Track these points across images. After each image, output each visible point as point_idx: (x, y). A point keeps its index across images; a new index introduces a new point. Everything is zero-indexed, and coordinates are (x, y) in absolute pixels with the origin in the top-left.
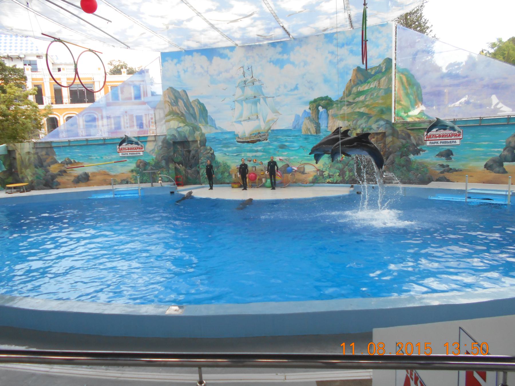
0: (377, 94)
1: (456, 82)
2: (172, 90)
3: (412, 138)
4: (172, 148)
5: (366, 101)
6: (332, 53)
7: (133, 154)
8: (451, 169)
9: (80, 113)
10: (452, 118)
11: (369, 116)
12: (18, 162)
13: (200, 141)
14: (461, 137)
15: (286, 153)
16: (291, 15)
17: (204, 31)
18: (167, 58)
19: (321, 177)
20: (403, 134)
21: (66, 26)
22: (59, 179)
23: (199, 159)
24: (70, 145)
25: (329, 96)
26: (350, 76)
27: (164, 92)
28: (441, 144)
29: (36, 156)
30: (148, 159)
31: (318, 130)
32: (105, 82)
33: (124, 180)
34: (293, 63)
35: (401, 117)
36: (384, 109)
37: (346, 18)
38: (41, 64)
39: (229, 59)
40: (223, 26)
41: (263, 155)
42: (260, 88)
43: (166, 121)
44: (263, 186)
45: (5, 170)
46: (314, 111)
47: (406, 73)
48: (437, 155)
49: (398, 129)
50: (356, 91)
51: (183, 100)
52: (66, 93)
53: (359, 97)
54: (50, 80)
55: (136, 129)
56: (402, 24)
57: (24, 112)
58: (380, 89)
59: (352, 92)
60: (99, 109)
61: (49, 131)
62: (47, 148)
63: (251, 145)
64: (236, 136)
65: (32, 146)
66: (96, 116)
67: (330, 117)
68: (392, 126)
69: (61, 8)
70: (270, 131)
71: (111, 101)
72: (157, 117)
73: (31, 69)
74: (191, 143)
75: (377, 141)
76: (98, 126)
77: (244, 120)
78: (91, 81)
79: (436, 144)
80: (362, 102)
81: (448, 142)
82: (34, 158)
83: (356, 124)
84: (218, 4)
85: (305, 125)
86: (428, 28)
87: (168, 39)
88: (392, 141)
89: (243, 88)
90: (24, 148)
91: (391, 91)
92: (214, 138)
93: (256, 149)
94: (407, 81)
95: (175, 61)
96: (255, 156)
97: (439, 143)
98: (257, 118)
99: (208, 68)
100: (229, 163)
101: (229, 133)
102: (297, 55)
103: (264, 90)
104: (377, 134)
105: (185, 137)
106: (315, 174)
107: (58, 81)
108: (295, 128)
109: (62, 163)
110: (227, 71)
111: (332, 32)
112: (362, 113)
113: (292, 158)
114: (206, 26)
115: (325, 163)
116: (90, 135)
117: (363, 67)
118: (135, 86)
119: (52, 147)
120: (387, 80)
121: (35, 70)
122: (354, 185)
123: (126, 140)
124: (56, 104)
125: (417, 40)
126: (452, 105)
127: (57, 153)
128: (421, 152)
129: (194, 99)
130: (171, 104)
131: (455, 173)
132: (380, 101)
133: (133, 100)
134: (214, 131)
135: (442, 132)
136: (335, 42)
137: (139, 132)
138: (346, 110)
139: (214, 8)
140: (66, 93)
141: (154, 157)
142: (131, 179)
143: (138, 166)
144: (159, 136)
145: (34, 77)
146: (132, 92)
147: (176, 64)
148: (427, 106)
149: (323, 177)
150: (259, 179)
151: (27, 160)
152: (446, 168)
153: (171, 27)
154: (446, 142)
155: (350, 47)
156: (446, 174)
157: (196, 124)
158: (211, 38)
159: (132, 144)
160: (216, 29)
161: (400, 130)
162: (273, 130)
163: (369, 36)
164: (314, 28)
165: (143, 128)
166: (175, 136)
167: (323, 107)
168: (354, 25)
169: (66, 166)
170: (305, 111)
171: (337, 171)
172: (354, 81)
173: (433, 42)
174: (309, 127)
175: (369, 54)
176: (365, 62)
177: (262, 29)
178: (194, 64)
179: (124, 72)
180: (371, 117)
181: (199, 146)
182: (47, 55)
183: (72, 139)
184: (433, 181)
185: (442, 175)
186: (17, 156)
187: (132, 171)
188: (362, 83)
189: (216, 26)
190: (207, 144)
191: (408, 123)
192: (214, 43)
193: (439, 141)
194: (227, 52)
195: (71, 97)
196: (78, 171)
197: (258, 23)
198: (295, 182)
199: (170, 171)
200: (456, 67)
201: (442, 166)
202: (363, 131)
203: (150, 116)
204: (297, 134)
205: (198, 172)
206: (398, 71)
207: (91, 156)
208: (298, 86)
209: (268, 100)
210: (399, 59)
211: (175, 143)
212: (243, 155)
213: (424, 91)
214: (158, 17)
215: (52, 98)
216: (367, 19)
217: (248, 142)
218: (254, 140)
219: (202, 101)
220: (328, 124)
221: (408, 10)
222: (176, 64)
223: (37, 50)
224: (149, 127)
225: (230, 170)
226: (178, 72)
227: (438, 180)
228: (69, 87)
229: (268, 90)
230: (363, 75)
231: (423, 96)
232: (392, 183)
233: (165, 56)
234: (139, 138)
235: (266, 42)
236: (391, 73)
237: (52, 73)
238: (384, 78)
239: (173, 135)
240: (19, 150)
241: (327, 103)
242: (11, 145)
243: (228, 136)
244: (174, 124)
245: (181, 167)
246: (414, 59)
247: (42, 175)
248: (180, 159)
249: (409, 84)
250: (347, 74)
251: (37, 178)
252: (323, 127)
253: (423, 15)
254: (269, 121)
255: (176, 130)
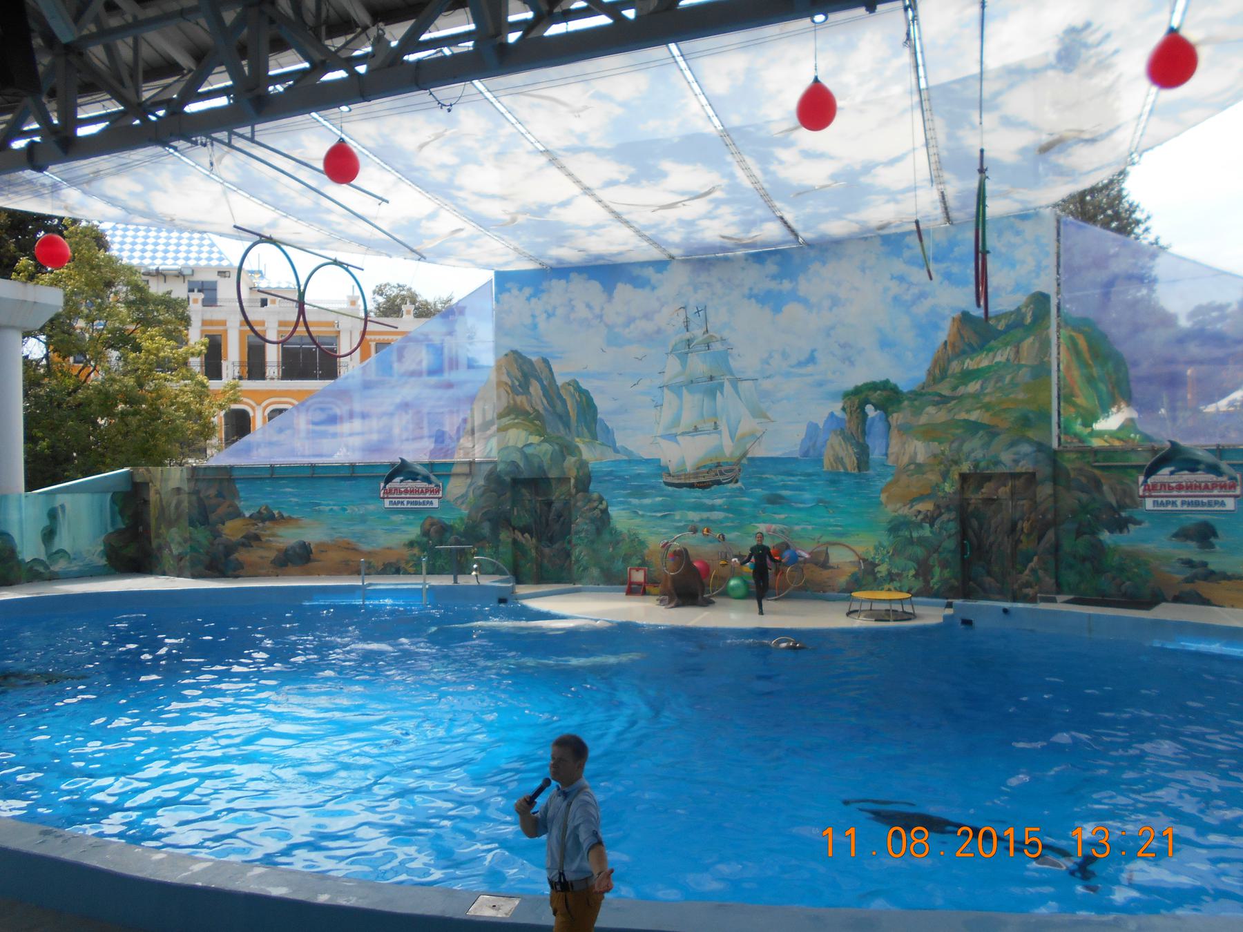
0: (1013, 379)
1: (1219, 353)
2: (516, 357)
3: (1105, 488)
4: (508, 494)
5: (985, 395)
6: (901, 279)
7: (416, 503)
8: (1212, 573)
9: (302, 404)
10: (1214, 442)
11: (991, 432)
12: (153, 511)
13: (576, 479)
14: (1238, 492)
15: (782, 516)
16: (802, 194)
17: (599, 226)
18: (508, 286)
19: (870, 578)
20: (1083, 480)
21: (288, 212)
22: (241, 555)
23: (570, 523)
24: (273, 475)
25: (893, 381)
26: (943, 335)
27: (498, 361)
28: (1185, 508)
29: (194, 498)
30: (448, 518)
31: (863, 460)
32: (364, 333)
33: (390, 564)
34: (804, 301)
35: (1076, 435)
36: (1031, 415)
37: (933, 202)
38: (226, 290)
39: (654, 288)
40: (643, 218)
41: (726, 518)
42: (724, 357)
43: (499, 430)
44: (725, 594)
45: (121, 525)
46: (854, 416)
47: (1086, 329)
48: (1176, 535)
49: (1068, 466)
50: (958, 370)
51: (540, 381)
52: (273, 354)
53: (966, 384)
54: (241, 325)
55: (429, 444)
56: (1072, 213)
57: (177, 396)
58: (1020, 367)
59: (950, 372)
60: (344, 394)
61: (229, 441)
62: (221, 480)
63: (698, 492)
64: (662, 469)
65: (185, 475)
66: (338, 411)
67: (894, 432)
68: (1054, 457)
69: (282, 172)
70: (744, 461)
71: (372, 376)
72: (478, 421)
73: (204, 300)
74: (553, 483)
75: (1013, 493)
76: (342, 435)
77: (683, 434)
78: (331, 329)
79: (1169, 508)
80: (976, 396)
81: (1203, 504)
82: (190, 502)
83: (959, 450)
84: (632, 170)
85: (832, 447)
86: (1138, 222)
87: (515, 244)
88: (1055, 496)
89: (683, 357)
90: (170, 478)
91: (1049, 372)
92: (610, 473)
93: (708, 502)
94: (1090, 347)
95: (528, 291)
96: (708, 520)
97: (1179, 503)
98: (716, 428)
99: (602, 309)
100: (643, 534)
101: (647, 462)
102: (817, 282)
103: (732, 363)
104: (1015, 476)
105: (541, 467)
106: (854, 569)
107: (257, 328)
108: (806, 454)
109: (251, 516)
110: (647, 316)
111: (898, 231)
112: (974, 423)
113: (797, 528)
114: (601, 214)
115: (881, 545)
116: (321, 456)
117: (979, 313)
118: (430, 346)
119: (231, 480)
120: (1037, 345)
121: (210, 301)
122: (957, 602)
123: (402, 470)
124: (249, 379)
125: (1112, 251)
126: (1211, 408)
127: (241, 494)
128: (1131, 527)
129: (567, 379)
130: (513, 387)
131: (1223, 582)
132: (1021, 396)
133: (426, 379)
134: (611, 456)
135: (1185, 477)
136: (907, 254)
137: (432, 453)
138: (932, 414)
139: (623, 178)
140: (273, 354)
141: (465, 512)
142: (407, 562)
143: (426, 533)
144: (481, 463)
145: (208, 317)
146: (424, 358)
147: (528, 299)
148: (1139, 412)
149: (875, 579)
150: (715, 577)
151: (173, 505)
152: (1199, 570)
153: (521, 219)
154: (1197, 504)
155: (944, 265)
156: (1198, 586)
157: (568, 438)
158: (616, 242)
159: (415, 479)
160: (626, 223)
161: (1074, 469)
162: (752, 459)
163: (992, 241)
164: (857, 222)
165: (443, 442)
166: (518, 466)
167: (876, 407)
168: (953, 214)
169: (261, 525)
170: (832, 415)
171: (911, 564)
172: (953, 346)
173: (1153, 256)
174: (842, 453)
175: (994, 280)
176: (982, 303)
177: (733, 224)
178: (571, 300)
179: (408, 312)
180: (998, 434)
181: (573, 491)
182: (240, 269)
183: (280, 460)
184: (1165, 600)
185: (1188, 587)
186: (153, 497)
187: (411, 544)
188: (974, 350)
189: (625, 217)
190: (592, 487)
191: (1095, 452)
192: (620, 254)
193: (1179, 501)
194: (649, 272)
195: (284, 364)
196: (287, 537)
197: (725, 210)
198: (804, 588)
199: (501, 549)
200: (1215, 314)
201: (1189, 563)
202: (976, 466)
203: (462, 416)
204: (810, 470)
205: (568, 555)
206: (1064, 322)
207: (319, 505)
208: (816, 354)
209: (743, 386)
210: (1065, 295)
211: (517, 483)
212: (677, 517)
213: (1133, 373)
214: (493, 197)
215: (241, 364)
216: (987, 203)
217: (692, 486)
218: (707, 479)
219: (584, 385)
220: (887, 446)
221: (1086, 184)
222: (528, 299)
223: (221, 259)
224: (458, 439)
225: (646, 551)
226: (533, 316)
227: (1177, 599)
228: (283, 342)
229: (746, 361)
230: (977, 331)
231: (1132, 385)
232: (1053, 600)
233: (504, 280)
234: (431, 466)
235: (740, 253)
236: (1048, 328)
237: (246, 309)
238: (1031, 339)
239: (513, 462)
240: (158, 484)
241: (884, 396)
242: (142, 470)
243: (643, 470)
244: (518, 437)
245: (527, 540)
246: (1106, 295)
247: (205, 542)
248: (526, 519)
249: (1095, 355)
250: (936, 327)
251: (193, 549)
252: (876, 455)
253: (1124, 193)
254: (743, 437)
255: (521, 450)
